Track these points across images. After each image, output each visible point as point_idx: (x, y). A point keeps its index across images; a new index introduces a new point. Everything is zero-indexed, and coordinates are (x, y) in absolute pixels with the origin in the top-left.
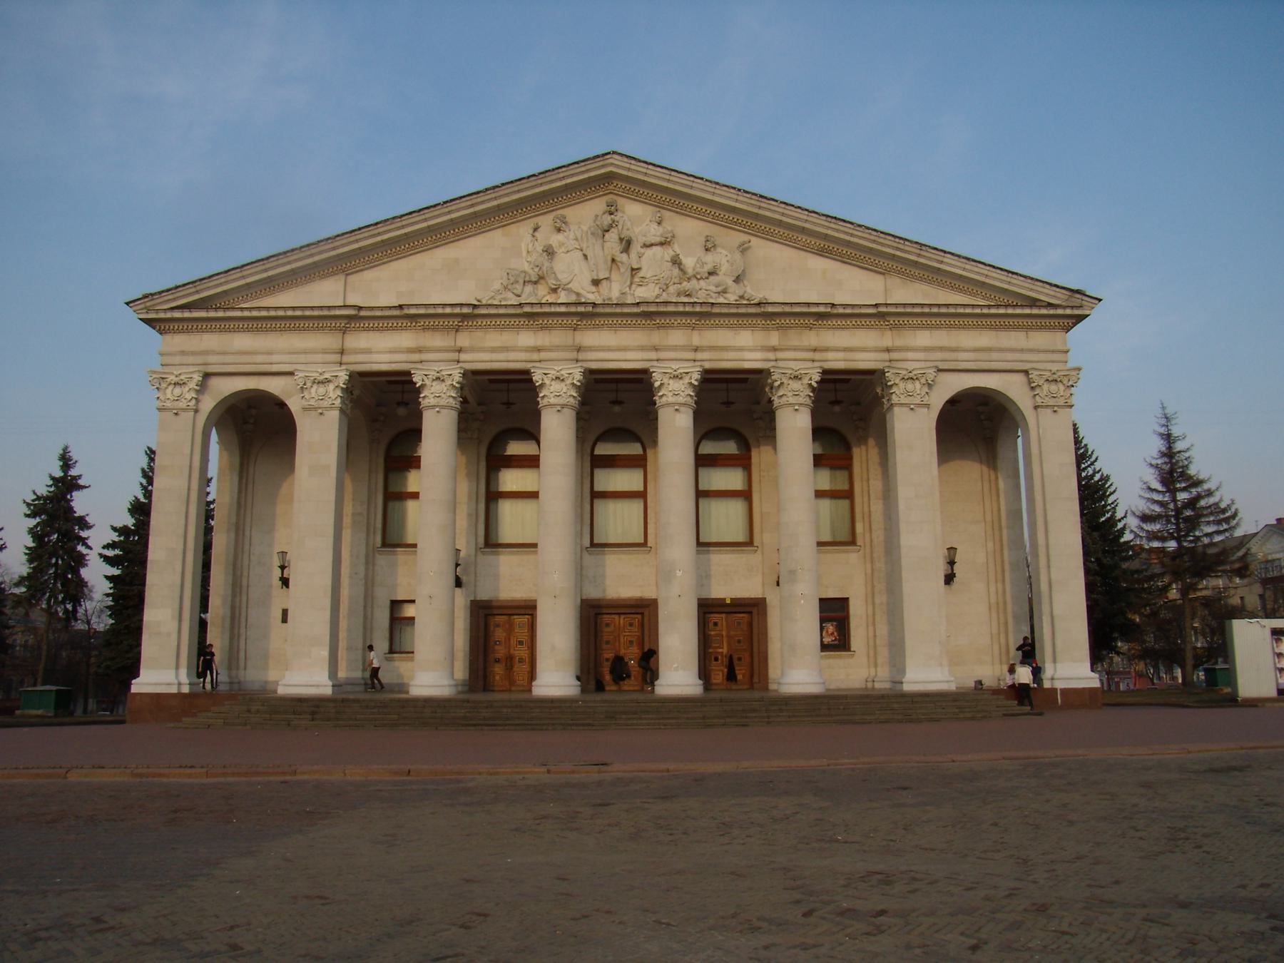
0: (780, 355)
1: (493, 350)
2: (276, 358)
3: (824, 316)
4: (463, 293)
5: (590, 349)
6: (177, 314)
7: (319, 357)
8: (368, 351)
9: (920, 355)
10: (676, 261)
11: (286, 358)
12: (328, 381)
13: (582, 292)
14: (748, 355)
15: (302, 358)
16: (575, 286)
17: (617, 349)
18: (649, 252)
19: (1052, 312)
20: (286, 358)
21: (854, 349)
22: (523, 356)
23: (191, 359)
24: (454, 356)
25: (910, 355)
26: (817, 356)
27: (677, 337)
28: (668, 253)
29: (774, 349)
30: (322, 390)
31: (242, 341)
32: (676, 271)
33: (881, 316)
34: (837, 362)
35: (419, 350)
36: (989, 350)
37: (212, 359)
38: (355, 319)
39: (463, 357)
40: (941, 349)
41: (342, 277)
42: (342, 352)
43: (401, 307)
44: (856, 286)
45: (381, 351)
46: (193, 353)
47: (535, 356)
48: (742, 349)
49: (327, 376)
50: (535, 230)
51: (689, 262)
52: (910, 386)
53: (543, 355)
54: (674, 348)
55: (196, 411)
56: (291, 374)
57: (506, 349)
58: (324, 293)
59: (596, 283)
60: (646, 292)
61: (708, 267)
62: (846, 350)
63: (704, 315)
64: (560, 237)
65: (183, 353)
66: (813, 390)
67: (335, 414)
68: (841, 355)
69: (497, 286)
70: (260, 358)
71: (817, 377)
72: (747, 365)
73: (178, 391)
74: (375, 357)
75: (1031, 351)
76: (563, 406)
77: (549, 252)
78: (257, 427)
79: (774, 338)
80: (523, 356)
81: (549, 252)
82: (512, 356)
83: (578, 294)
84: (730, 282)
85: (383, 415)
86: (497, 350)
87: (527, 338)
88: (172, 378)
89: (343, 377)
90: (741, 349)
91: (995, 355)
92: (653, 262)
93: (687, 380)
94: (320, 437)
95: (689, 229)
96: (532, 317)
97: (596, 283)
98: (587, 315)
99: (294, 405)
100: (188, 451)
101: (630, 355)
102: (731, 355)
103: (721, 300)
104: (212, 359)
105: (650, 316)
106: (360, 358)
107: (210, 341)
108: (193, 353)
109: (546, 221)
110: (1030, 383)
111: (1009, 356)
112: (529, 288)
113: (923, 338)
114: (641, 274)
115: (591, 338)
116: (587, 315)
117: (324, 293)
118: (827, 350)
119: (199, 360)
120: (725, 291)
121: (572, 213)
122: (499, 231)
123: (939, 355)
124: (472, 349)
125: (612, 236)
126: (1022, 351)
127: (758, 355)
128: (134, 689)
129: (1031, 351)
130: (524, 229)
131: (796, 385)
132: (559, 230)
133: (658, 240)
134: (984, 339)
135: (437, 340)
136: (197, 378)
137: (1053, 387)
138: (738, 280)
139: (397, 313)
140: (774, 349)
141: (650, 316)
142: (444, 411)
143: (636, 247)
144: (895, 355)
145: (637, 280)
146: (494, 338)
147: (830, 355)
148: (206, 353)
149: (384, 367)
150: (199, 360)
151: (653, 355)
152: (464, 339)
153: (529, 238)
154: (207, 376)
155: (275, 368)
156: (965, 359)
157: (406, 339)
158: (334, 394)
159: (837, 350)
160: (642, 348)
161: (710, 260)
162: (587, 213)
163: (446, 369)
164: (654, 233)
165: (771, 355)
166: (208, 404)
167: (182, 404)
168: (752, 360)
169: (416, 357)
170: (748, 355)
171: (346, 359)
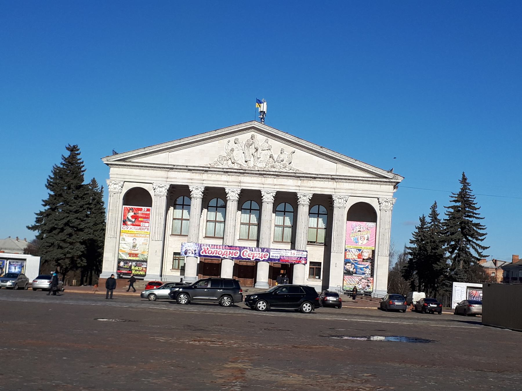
0: (300, 188)
1: (214, 181)
2: (147, 178)
5: (243, 183)
7: (160, 179)
8: (175, 178)
9: (345, 191)
11: (150, 178)
13: (242, 164)
14: (291, 188)
15: (155, 179)
17: (251, 183)
19: (387, 180)
20: (150, 178)
22: (223, 183)
24: (202, 182)
25: (342, 191)
26: (312, 189)
27: (270, 180)
28: (269, 153)
30: (161, 189)
32: (271, 159)
38: (172, 168)
39: (204, 182)
40: (351, 189)
45: (180, 178)
46: (121, 175)
48: (289, 185)
49: (163, 185)
51: (275, 157)
53: (229, 184)
54: (269, 184)
57: (218, 181)
59: (246, 162)
60: (260, 165)
61: (281, 159)
63: (277, 175)
66: (310, 200)
69: (216, 159)
70: (141, 178)
73: (115, 186)
74: (178, 180)
76: (234, 200)
77: (232, 150)
79: (299, 182)
80: (223, 183)
83: (241, 165)
88: (113, 182)
89: (168, 187)
91: (369, 192)
92: (264, 155)
93: (272, 194)
98: (243, 172)
99: (152, 193)
102: (285, 187)
105: (262, 174)
106: (173, 180)
108: (121, 175)
109: (232, 139)
110: (379, 202)
112: (225, 162)
118: (315, 187)
119: (123, 177)
120: (286, 167)
123: (350, 191)
127: (294, 188)
128: (101, 277)
131: (305, 198)
132: (235, 143)
135: (196, 176)
136: (122, 183)
137: (387, 204)
143: (260, 150)
145: (259, 161)
147: (316, 189)
150: (123, 177)
151: (262, 186)
157: (188, 175)
158: (164, 192)
161: (282, 157)
163: (199, 186)
164: (266, 146)
165: (298, 188)
166: (125, 191)
170: (291, 188)
171: (168, 180)
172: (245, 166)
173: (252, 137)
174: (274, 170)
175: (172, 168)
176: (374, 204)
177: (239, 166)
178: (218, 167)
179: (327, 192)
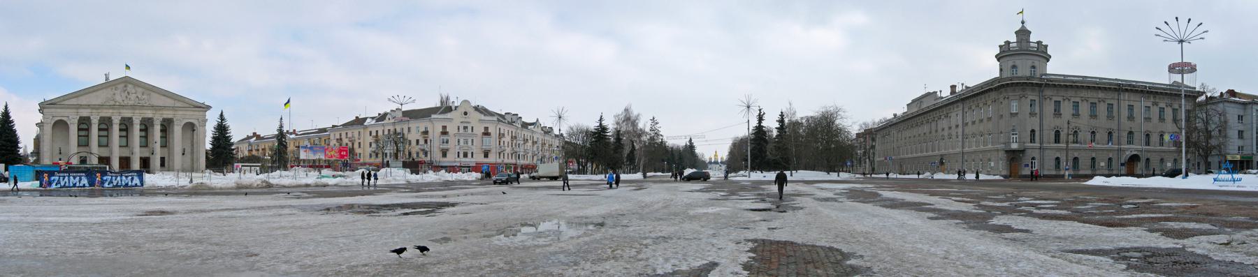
17: (127, 113)
21: (168, 114)
33: (174, 108)
44: (169, 102)
45: (85, 113)
58: (74, 101)
60: (131, 103)
78: (61, 125)
85: (84, 124)
86: (106, 113)
92: (133, 97)
94: (74, 129)
95: (140, 90)
96: (112, 107)
105: (133, 107)
117: (74, 101)
141: (133, 107)
176: (195, 122)
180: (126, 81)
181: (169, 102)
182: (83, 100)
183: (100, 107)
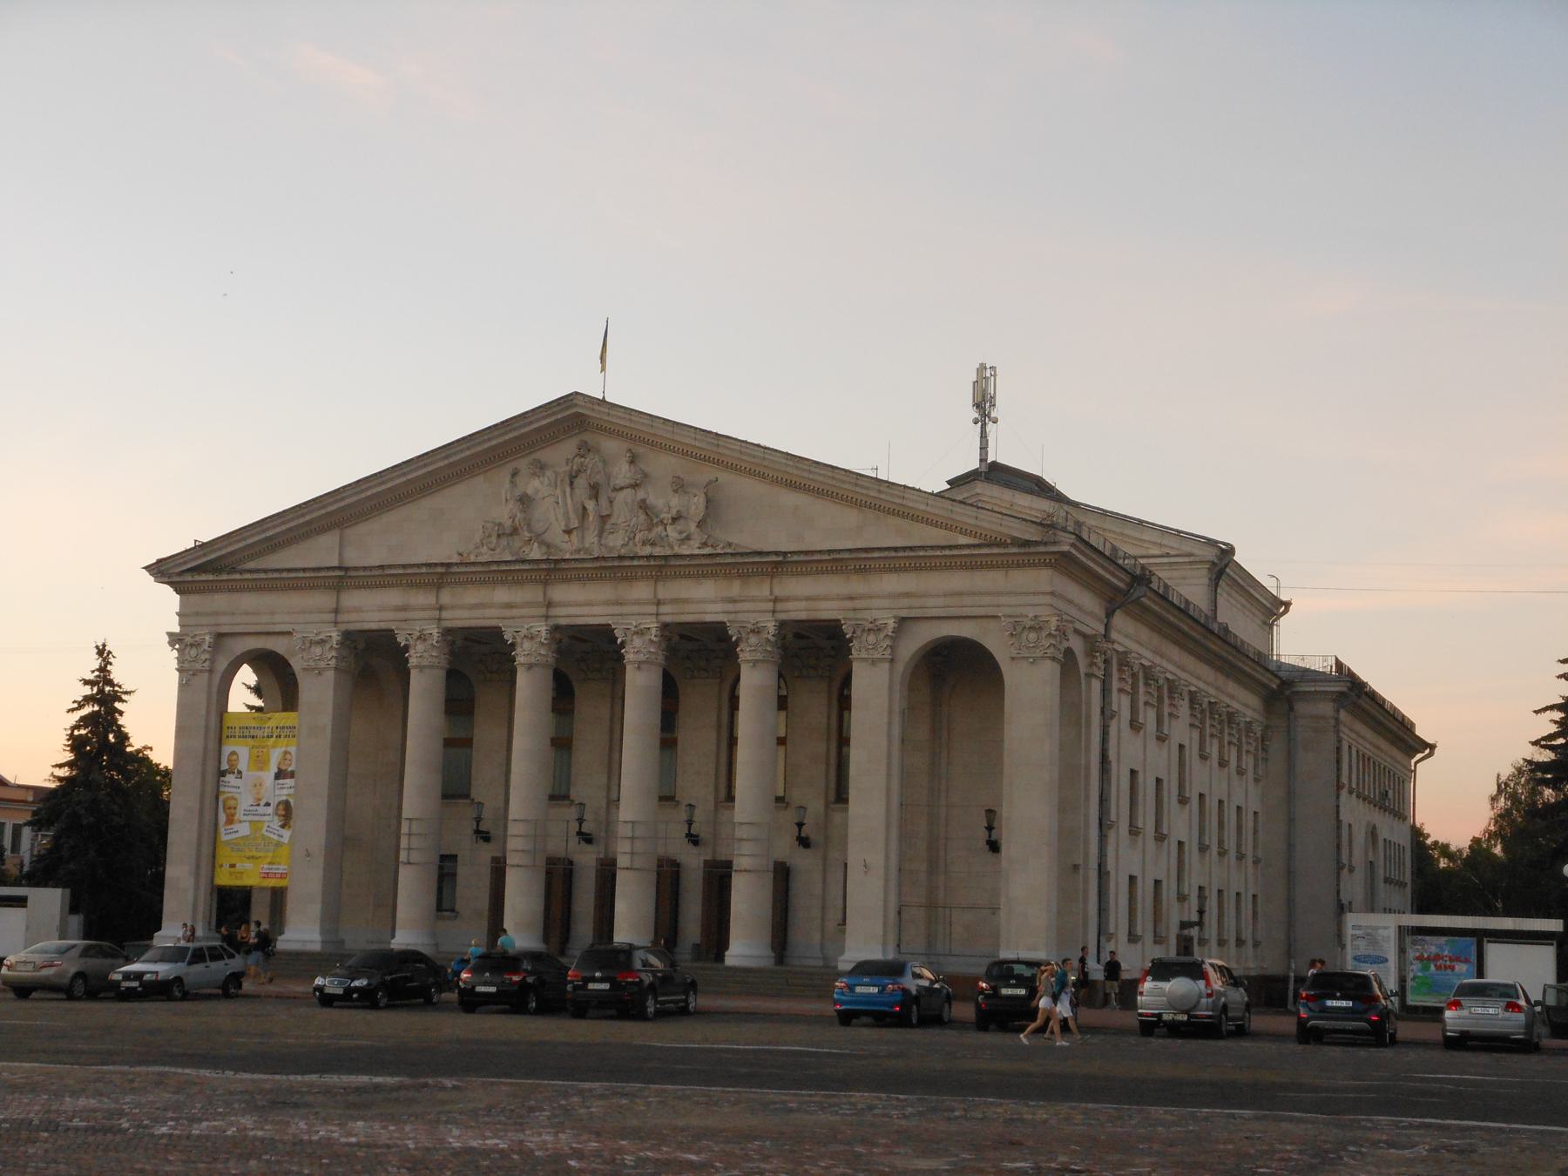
0: (739, 606)
3: (778, 564)
4: (442, 550)
6: (188, 578)
8: (358, 610)
9: (886, 603)
10: (644, 506)
12: (322, 642)
16: (547, 537)
18: (621, 497)
21: (815, 597)
23: (204, 620)
26: (779, 606)
27: (641, 591)
29: (733, 601)
31: (249, 601)
32: (642, 517)
34: (798, 611)
35: (404, 608)
36: (960, 594)
37: (223, 619)
38: (342, 578)
39: (445, 614)
40: (907, 595)
41: (337, 532)
42: (336, 611)
43: (382, 567)
45: (371, 609)
47: (507, 613)
48: (704, 601)
50: (515, 474)
52: (872, 638)
53: (515, 612)
54: (637, 602)
55: (211, 671)
56: (289, 633)
58: (321, 552)
60: (616, 541)
62: (808, 599)
63: (663, 568)
64: (536, 483)
65: (197, 614)
67: (331, 674)
68: (803, 604)
70: (264, 619)
71: (772, 630)
72: (708, 618)
75: (1009, 593)
79: (735, 588)
81: (525, 501)
82: (488, 612)
83: (548, 546)
84: (693, 527)
86: (472, 607)
87: (502, 595)
89: (336, 636)
90: (703, 601)
91: (967, 600)
97: (568, 532)
98: (553, 570)
100: (203, 712)
101: (597, 610)
103: (685, 550)
104: (223, 619)
106: (354, 617)
107: (220, 601)
109: (523, 464)
111: (987, 600)
112: (504, 542)
113: (891, 583)
114: (613, 520)
115: (560, 593)
116: (553, 570)
117: (321, 552)
119: (212, 620)
120: (688, 538)
121: (546, 455)
122: (481, 479)
123: (906, 602)
124: (453, 607)
125: (581, 482)
126: (999, 594)
127: (719, 607)
129: (1009, 593)
130: (502, 476)
131: (753, 640)
133: (628, 482)
134: (958, 580)
138: (699, 525)
139: (379, 572)
140: (733, 601)
142: (427, 671)
144: (858, 604)
146: (472, 596)
147: (790, 605)
148: (216, 614)
149: (374, 626)
150: (212, 620)
152: (446, 597)
153: (507, 485)
154: (220, 636)
155: (278, 628)
156: (934, 606)
157: (393, 597)
159: (796, 599)
160: (607, 603)
161: (676, 502)
162: (561, 454)
165: (730, 607)
167: (198, 666)
168: (713, 613)
169: (402, 615)
171: (341, 618)
172: (567, 547)
173: (585, 449)
174: (647, 550)
175: (342, 578)
177: (544, 549)
178: (480, 559)
179: (827, 611)
180: (572, 420)
181: (831, 528)
182: (372, 545)
183: (440, 576)
